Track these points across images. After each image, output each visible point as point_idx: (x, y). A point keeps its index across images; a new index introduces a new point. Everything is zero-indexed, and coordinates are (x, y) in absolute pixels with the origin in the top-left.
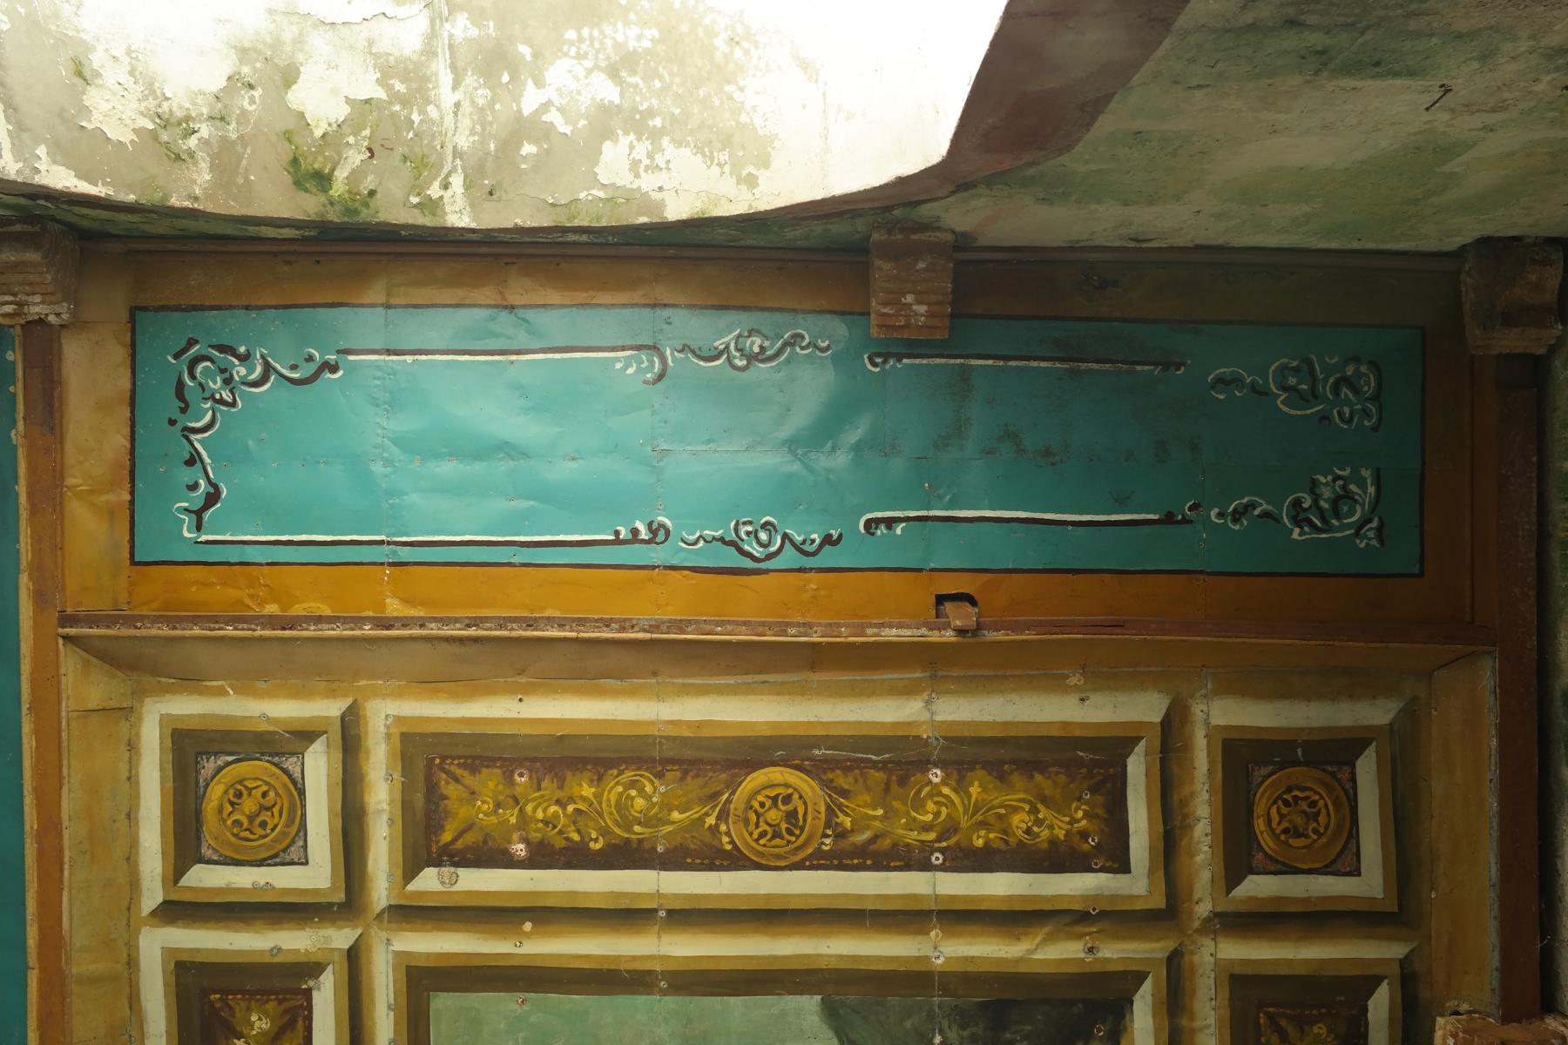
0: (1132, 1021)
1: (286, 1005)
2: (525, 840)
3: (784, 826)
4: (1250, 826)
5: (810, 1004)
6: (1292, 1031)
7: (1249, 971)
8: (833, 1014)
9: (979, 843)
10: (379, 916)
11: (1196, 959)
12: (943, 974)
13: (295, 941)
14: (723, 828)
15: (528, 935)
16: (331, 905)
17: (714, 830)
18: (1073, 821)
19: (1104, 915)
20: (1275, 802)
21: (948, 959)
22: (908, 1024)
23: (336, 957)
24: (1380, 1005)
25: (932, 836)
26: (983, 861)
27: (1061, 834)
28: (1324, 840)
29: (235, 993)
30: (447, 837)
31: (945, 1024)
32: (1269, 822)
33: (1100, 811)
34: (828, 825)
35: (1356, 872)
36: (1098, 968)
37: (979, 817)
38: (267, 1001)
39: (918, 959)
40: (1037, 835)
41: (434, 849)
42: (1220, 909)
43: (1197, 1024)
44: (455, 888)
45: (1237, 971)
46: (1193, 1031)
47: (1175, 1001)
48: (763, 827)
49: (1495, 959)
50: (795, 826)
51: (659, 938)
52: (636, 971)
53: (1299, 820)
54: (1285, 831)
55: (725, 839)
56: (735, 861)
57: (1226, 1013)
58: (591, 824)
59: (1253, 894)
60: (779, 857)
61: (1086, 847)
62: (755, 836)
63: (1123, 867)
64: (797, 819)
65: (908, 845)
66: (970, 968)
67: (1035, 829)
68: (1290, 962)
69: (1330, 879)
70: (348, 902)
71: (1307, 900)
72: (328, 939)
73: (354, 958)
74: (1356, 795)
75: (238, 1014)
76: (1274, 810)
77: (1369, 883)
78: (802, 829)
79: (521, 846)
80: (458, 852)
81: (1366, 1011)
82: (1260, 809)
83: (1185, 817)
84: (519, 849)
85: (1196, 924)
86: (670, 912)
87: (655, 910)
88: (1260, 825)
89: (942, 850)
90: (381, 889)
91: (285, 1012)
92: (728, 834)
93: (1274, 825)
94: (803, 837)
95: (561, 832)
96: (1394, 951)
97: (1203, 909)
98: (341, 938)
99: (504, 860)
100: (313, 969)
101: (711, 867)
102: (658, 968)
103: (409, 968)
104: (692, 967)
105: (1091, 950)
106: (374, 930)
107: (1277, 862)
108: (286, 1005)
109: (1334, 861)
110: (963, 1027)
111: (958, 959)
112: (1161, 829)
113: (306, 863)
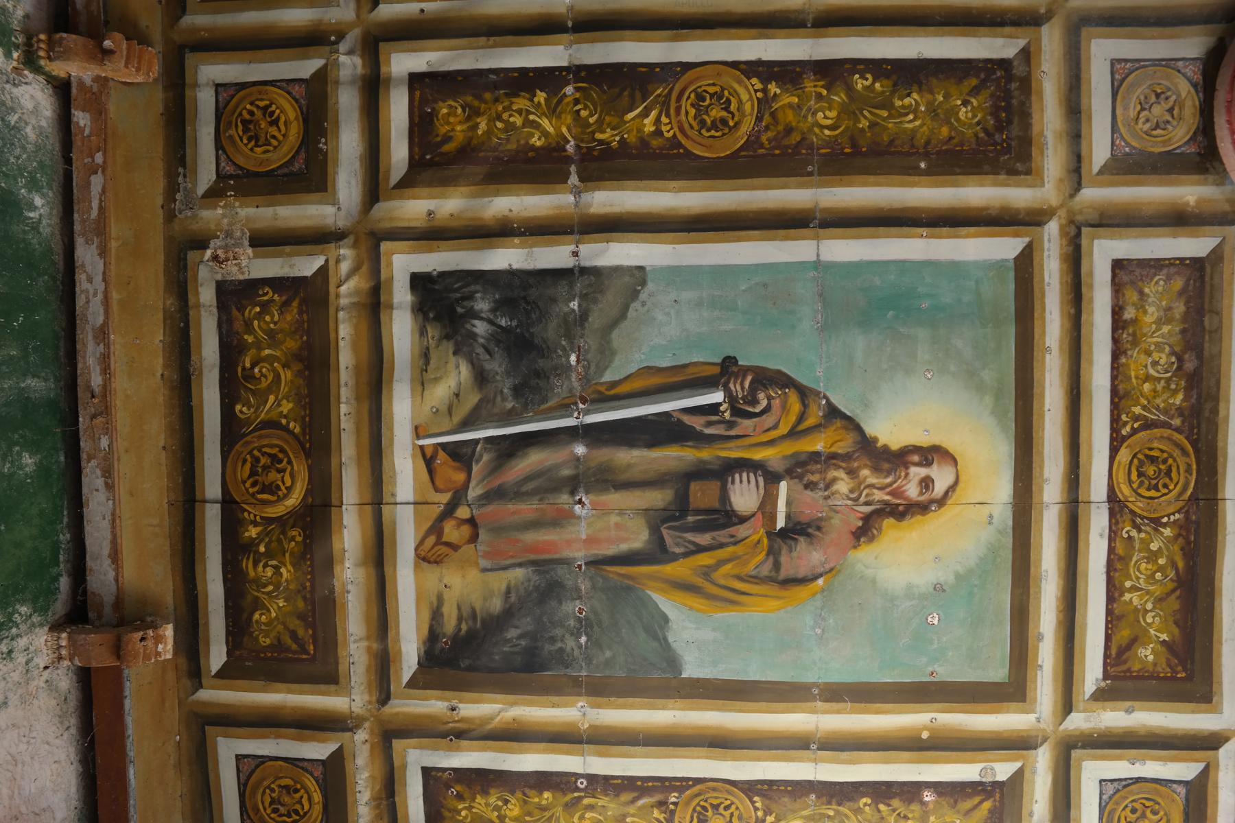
0: (419, 649)
1: (1124, 667)
2: (923, 804)
3: (710, 813)
4: (325, 797)
5: (692, 669)
6: (288, 641)
7: (323, 687)
8: (672, 662)
9: (546, 795)
10: (1045, 740)
11: (366, 698)
12: (580, 695)
13: (1114, 718)
14: (760, 814)
15: (926, 728)
16: (1083, 747)
17: (768, 812)
18: (470, 808)
19: (444, 735)
20: (305, 814)
21: (573, 705)
22: (608, 654)
23: (1081, 706)
24: (217, 656)
25: (586, 801)
26: (543, 780)
27: (479, 799)
28: (266, 783)
29: (1165, 678)
30: (987, 805)
31: (576, 652)
32: (310, 799)
33: (446, 814)
34: (673, 812)
35: (239, 758)
36: (448, 694)
37: (547, 814)
38: (1138, 671)
39: (599, 707)
40: (498, 799)
41: (998, 795)
42: (348, 734)
43: (365, 644)
44: (982, 765)
45: (333, 687)
46: (368, 638)
47: (383, 664)
48: (727, 814)
49: (127, 703)
50: (700, 813)
51: (817, 727)
52: (838, 701)
53: (286, 799)
54: (296, 791)
55: (758, 805)
56: (750, 788)
57: (342, 653)
58: (869, 817)
59: (322, 745)
60: (714, 789)
61: (459, 788)
62: (733, 807)
63: (426, 771)
64: (698, 818)
65: (606, 795)
66: (555, 699)
67: (500, 803)
68: (290, 692)
69: (260, 753)
70: (1069, 749)
71: (278, 737)
72: (1087, 720)
73: (1067, 706)
74: (242, 815)
75: (1164, 660)
76: (306, 807)
77: (229, 749)
78: (694, 810)
79: (926, 799)
80: (978, 794)
81: (228, 653)
82: (317, 810)
83: (378, 807)
84: (928, 797)
85: (367, 725)
86: (807, 748)
87: (818, 749)
88: (317, 797)
89: (577, 789)
90: (1043, 760)
91: (1125, 662)
92: (756, 809)
93: (306, 796)
94: (694, 803)
95: (894, 811)
96: (205, 695)
97: (361, 736)
98: (1077, 722)
99: (940, 788)
100: (1101, 696)
101: (771, 783)
102: (819, 704)
103: (1024, 700)
104: (791, 705)
105: (453, 709)
106: (1047, 724)
107: (302, 768)
108: (1124, 667)
109: (257, 766)
110: (561, 650)
111: (565, 705)
112: (397, 799)
113: (1101, 781)
